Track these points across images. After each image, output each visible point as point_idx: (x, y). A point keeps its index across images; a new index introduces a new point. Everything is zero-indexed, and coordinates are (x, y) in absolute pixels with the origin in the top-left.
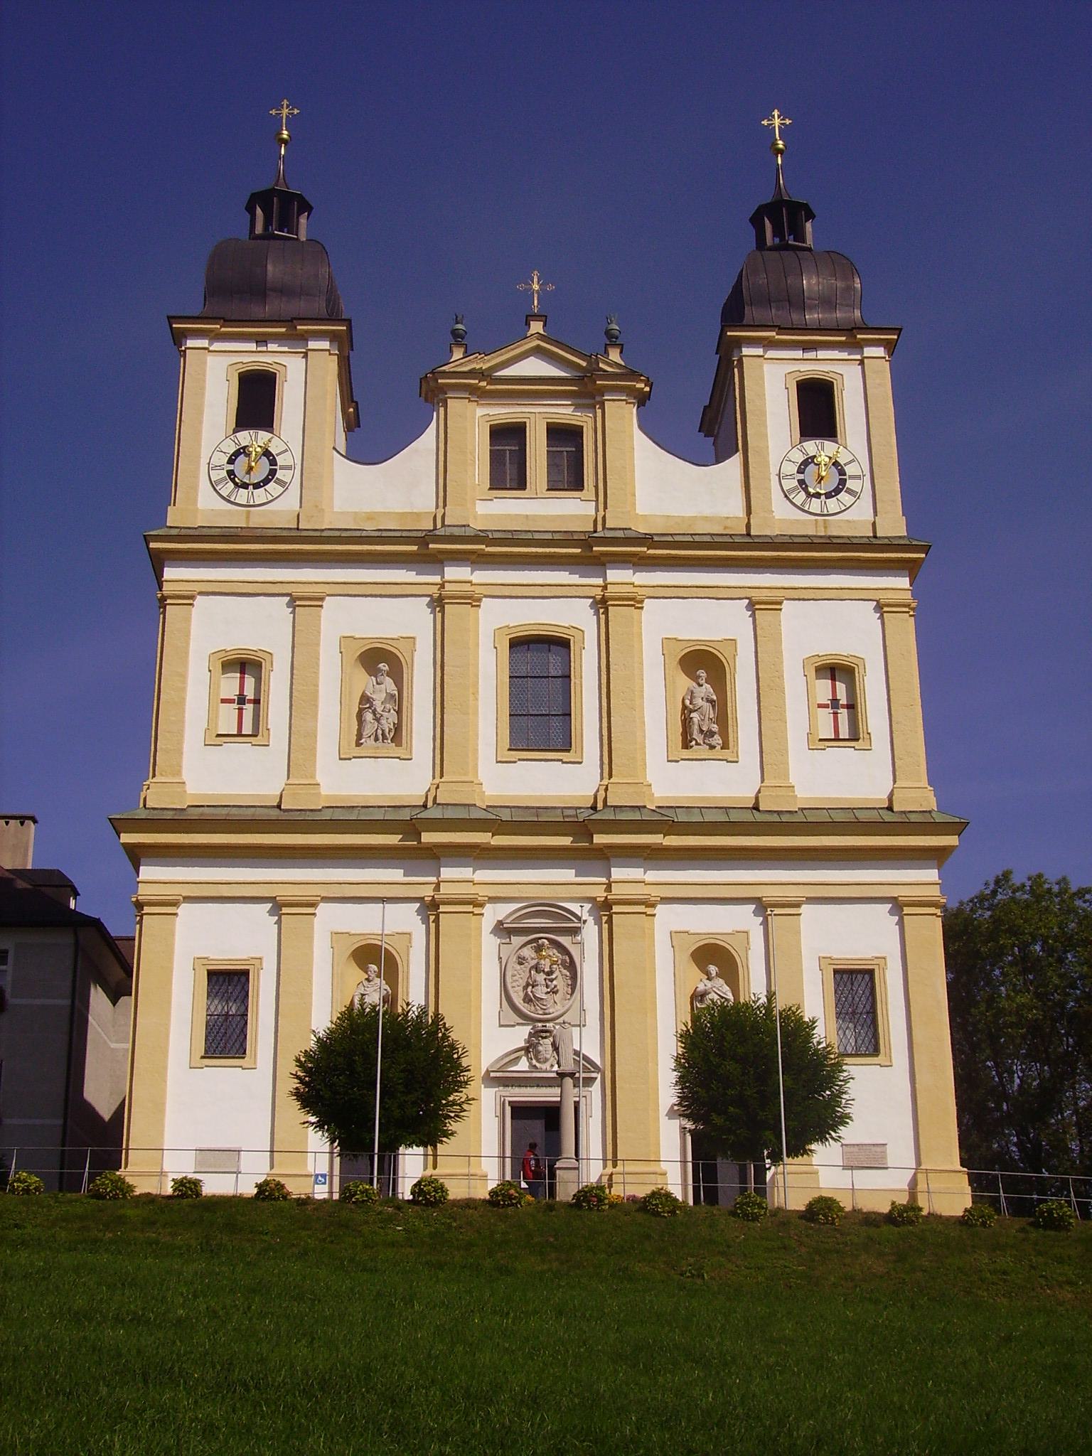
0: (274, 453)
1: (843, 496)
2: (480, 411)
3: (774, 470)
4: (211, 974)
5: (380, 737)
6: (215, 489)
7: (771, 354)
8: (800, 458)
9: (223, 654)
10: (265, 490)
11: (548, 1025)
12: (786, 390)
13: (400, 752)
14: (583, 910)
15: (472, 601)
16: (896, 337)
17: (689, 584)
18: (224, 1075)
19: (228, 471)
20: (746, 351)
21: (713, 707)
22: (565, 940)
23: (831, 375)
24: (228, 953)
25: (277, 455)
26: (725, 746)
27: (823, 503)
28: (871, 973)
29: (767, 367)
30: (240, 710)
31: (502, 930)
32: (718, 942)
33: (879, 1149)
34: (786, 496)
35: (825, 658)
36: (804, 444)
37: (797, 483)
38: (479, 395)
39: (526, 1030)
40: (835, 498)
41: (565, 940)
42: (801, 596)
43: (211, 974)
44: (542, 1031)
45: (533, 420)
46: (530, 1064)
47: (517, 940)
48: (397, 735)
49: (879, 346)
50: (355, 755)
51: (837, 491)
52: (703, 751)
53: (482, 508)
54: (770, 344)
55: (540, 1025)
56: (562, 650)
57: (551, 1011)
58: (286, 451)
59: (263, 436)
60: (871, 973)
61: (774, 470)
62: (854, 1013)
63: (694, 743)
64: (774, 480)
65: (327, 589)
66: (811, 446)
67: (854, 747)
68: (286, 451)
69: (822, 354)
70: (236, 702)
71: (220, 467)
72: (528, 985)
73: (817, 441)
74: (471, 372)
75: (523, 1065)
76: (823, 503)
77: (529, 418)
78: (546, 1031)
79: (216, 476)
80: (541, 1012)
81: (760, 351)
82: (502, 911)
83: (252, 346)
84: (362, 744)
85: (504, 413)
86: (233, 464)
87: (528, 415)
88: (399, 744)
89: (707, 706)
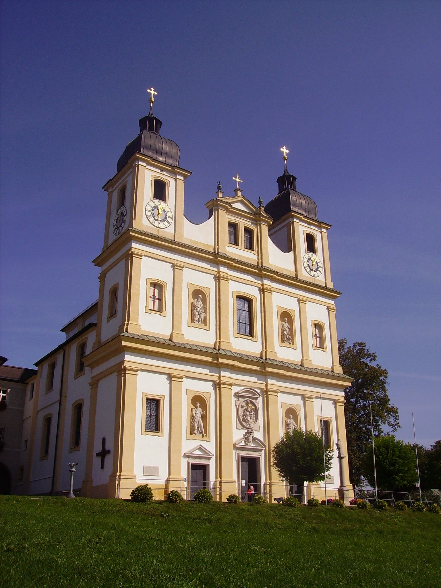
0: (166, 211)
2: (227, 216)
4: (148, 399)
6: (147, 218)
13: (205, 327)
15: (227, 279)
18: (152, 438)
22: (254, 401)
26: (293, 344)
30: (154, 301)
32: (293, 407)
34: (305, 268)
35: (316, 321)
38: (227, 211)
42: (312, 301)
43: (148, 399)
45: (240, 223)
48: (204, 321)
50: (193, 326)
52: (287, 344)
67: (323, 351)
69: (312, 227)
83: (159, 171)
87: (239, 222)
88: (206, 325)
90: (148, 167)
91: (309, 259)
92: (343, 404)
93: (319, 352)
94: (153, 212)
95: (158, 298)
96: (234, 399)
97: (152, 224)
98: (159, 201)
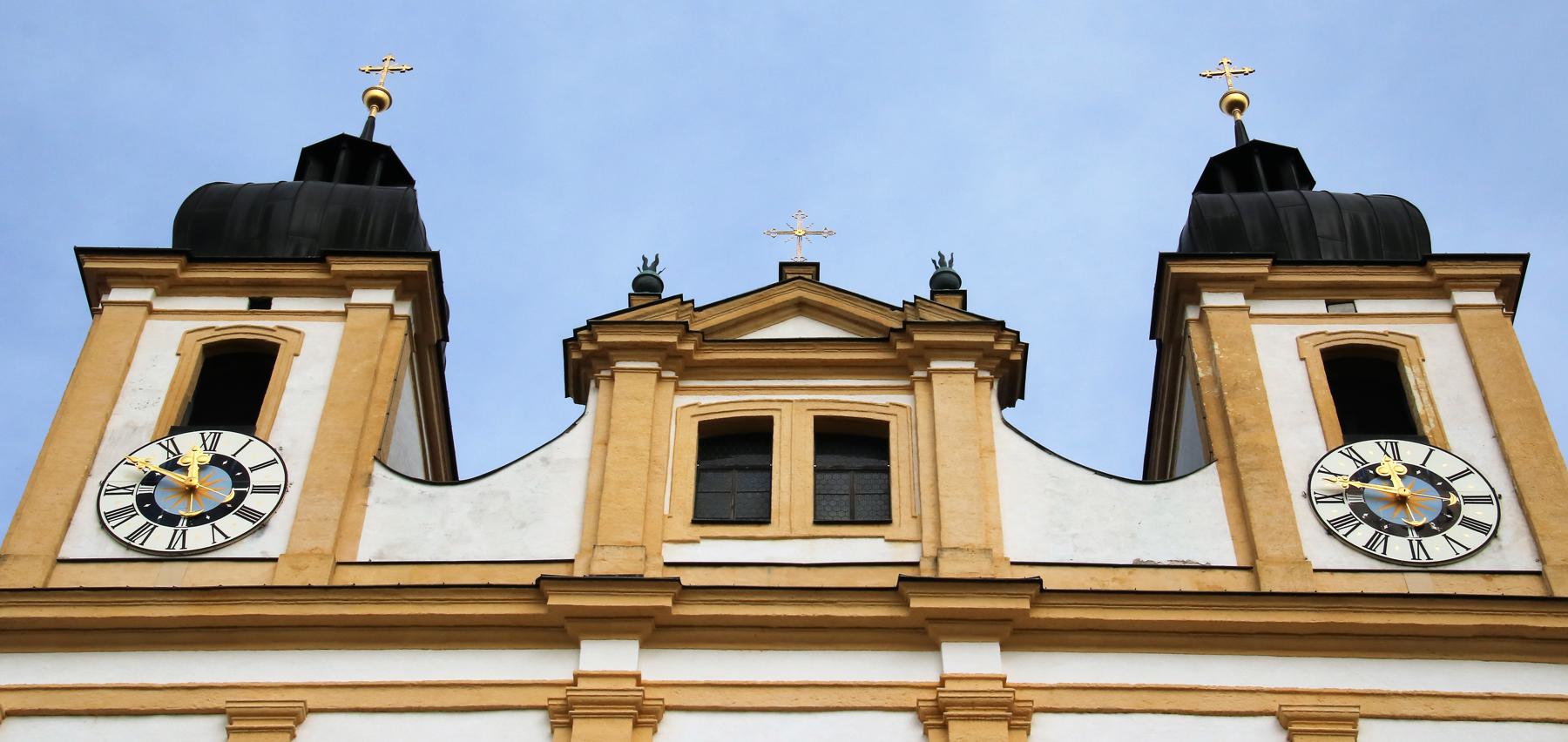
1: (1456, 531)
3: (1296, 486)
7: (1260, 307)
10: (213, 526)
12: (1303, 362)
16: (1517, 272)
17: (1133, 682)
20: (1209, 299)
23: (1391, 338)
25: (253, 469)
27: (1415, 544)
29: (1259, 330)
34: (1330, 532)
36: (1355, 446)
54: (1258, 289)
58: (274, 462)
61: (1296, 486)
64: (1301, 507)
66: (1369, 450)
68: (274, 462)
69: (1364, 306)
73: (1383, 442)
76: (1415, 544)
77: (780, 410)
81: (1237, 299)
87: (776, 405)
91: (1367, 473)
97: (129, 547)
98: (207, 433)
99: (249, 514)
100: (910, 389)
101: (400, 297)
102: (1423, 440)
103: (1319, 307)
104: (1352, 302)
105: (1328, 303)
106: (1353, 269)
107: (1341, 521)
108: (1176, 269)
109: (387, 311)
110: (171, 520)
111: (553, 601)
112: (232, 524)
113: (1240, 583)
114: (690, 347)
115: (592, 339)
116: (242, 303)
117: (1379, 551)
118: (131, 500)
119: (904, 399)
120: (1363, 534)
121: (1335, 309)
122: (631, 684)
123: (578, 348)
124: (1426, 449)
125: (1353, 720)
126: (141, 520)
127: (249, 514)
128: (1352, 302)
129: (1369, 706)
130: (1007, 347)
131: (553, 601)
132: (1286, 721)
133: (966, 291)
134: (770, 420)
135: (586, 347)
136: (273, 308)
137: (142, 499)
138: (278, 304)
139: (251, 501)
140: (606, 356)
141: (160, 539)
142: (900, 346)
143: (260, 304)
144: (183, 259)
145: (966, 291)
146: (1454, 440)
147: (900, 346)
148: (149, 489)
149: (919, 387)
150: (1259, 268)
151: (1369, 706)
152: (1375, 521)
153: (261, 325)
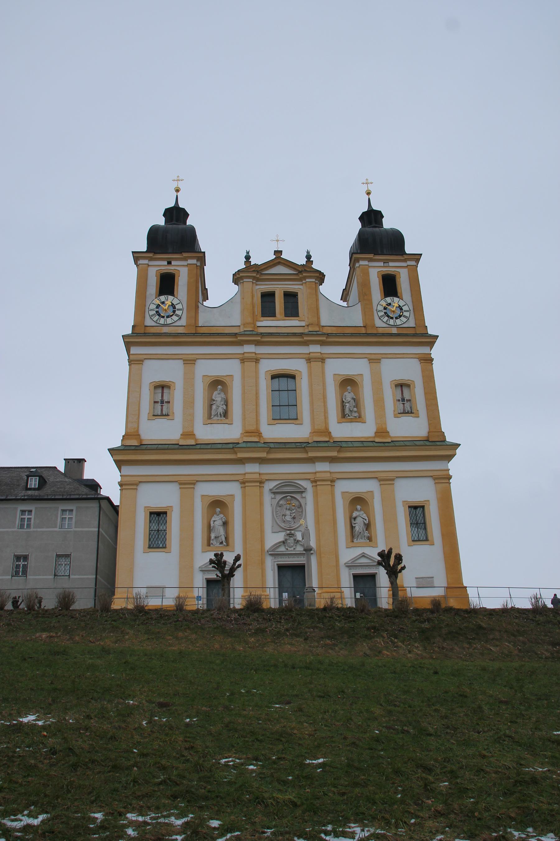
1: (402, 318)
2: (258, 287)
5: (219, 415)
8: (384, 304)
9: (154, 383)
11: (292, 532)
13: (227, 421)
14: (304, 484)
18: (157, 556)
19: (156, 311)
21: (355, 401)
22: (297, 496)
23: (395, 272)
24: (158, 504)
28: (423, 507)
30: (162, 406)
31: (274, 492)
33: (430, 579)
34: (380, 318)
35: (398, 381)
36: (386, 299)
37: (384, 314)
39: (283, 534)
40: (399, 319)
41: (297, 496)
43: (151, 513)
44: (290, 534)
46: (285, 548)
47: (279, 497)
48: (225, 414)
49: (414, 261)
51: (400, 316)
53: (259, 324)
55: (289, 532)
56: (293, 380)
57: (293, 526)
58: (179, 303)
59: (170, 298)
60: (423, 507)
61: (375, 308)
62: (417, 524)
63: (347, 415)
65: (197, 357)
66: (389, 300)
68: (179, 303)
69: (391, 264)
70: (160, 402)
71: (153, 310)
72: (283, 515)
74: (254, 271)
75: (282, 549)
78: (291, 534)
79: (152, 313)
80: (289, 527)
82: (272, 484)
84: (212, 418)
85: (266, 287)
86: (158, 308)
89: (352, 401)
90: (152, 263)
92: (330, 482)
93: (407, 420)
94: (157, 310)
95: (167, 401)
96: (267, 498)
98: (165, 296)
99: (177, 315)
100: (302, 284)
101: (197, 261)
102: (398, 297)
103: (381, 264)
104: (388, 263)
105: (384, 263)
106: (389, 256)
107: (382, 316)
108: (355, 256)
109: (196, 265)
110: (163, 317)
111: (239, 338)
112: (175, 318)
113: (363, 331)
114: (258, 276)
115: (239, 274)
116: (166, 263)
117: (388, 323)
118: (154, 312)
119: (301, 287)
120: (386, 318)
121: (386, 265)
122: (254, 355)
123: (236, 276)
124: (399, 299)
125: (380, 360)
126: (157, 317)
127: (177, 315)
128: (388, 263)
129: (384, 356)
130: (321, 276)
131: (239, 338)
132: (369, 360)
133: (313, 261)
134: (275, 291)
135: (238, 276)
136: (172, 264)
137: (157, 312)
138: (173, 263)
139: (177, 312)
140: (242, 278)
141: (162, 321)
142: (300, 276)
143: (169, 263)
144: (153, 253)
145: (313, 261)
146: (404, 298)
147: (300, 276)
148: (157, 310)
149: (304, 284)
150: (371, 256)
151: (384, 356)
152: (388, 316)
153: (170, 269)
